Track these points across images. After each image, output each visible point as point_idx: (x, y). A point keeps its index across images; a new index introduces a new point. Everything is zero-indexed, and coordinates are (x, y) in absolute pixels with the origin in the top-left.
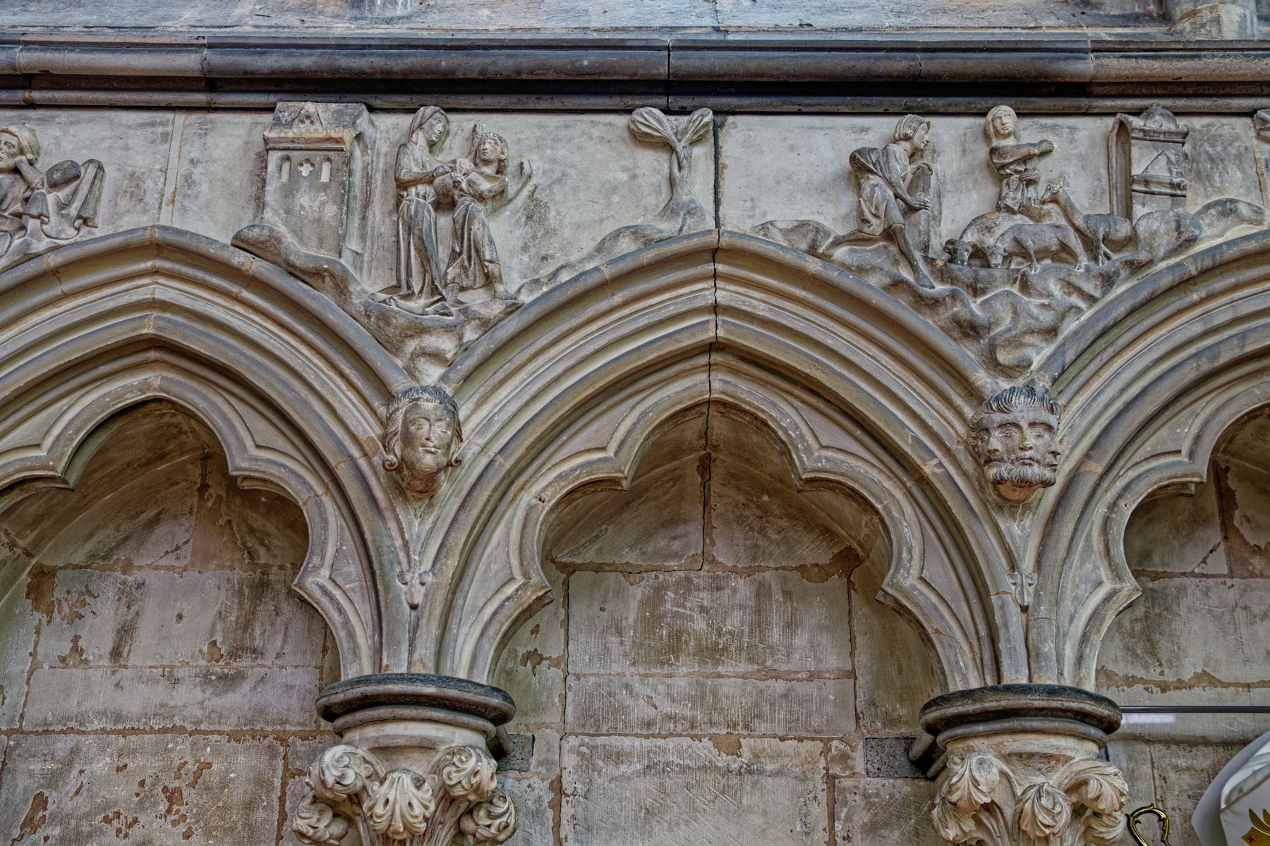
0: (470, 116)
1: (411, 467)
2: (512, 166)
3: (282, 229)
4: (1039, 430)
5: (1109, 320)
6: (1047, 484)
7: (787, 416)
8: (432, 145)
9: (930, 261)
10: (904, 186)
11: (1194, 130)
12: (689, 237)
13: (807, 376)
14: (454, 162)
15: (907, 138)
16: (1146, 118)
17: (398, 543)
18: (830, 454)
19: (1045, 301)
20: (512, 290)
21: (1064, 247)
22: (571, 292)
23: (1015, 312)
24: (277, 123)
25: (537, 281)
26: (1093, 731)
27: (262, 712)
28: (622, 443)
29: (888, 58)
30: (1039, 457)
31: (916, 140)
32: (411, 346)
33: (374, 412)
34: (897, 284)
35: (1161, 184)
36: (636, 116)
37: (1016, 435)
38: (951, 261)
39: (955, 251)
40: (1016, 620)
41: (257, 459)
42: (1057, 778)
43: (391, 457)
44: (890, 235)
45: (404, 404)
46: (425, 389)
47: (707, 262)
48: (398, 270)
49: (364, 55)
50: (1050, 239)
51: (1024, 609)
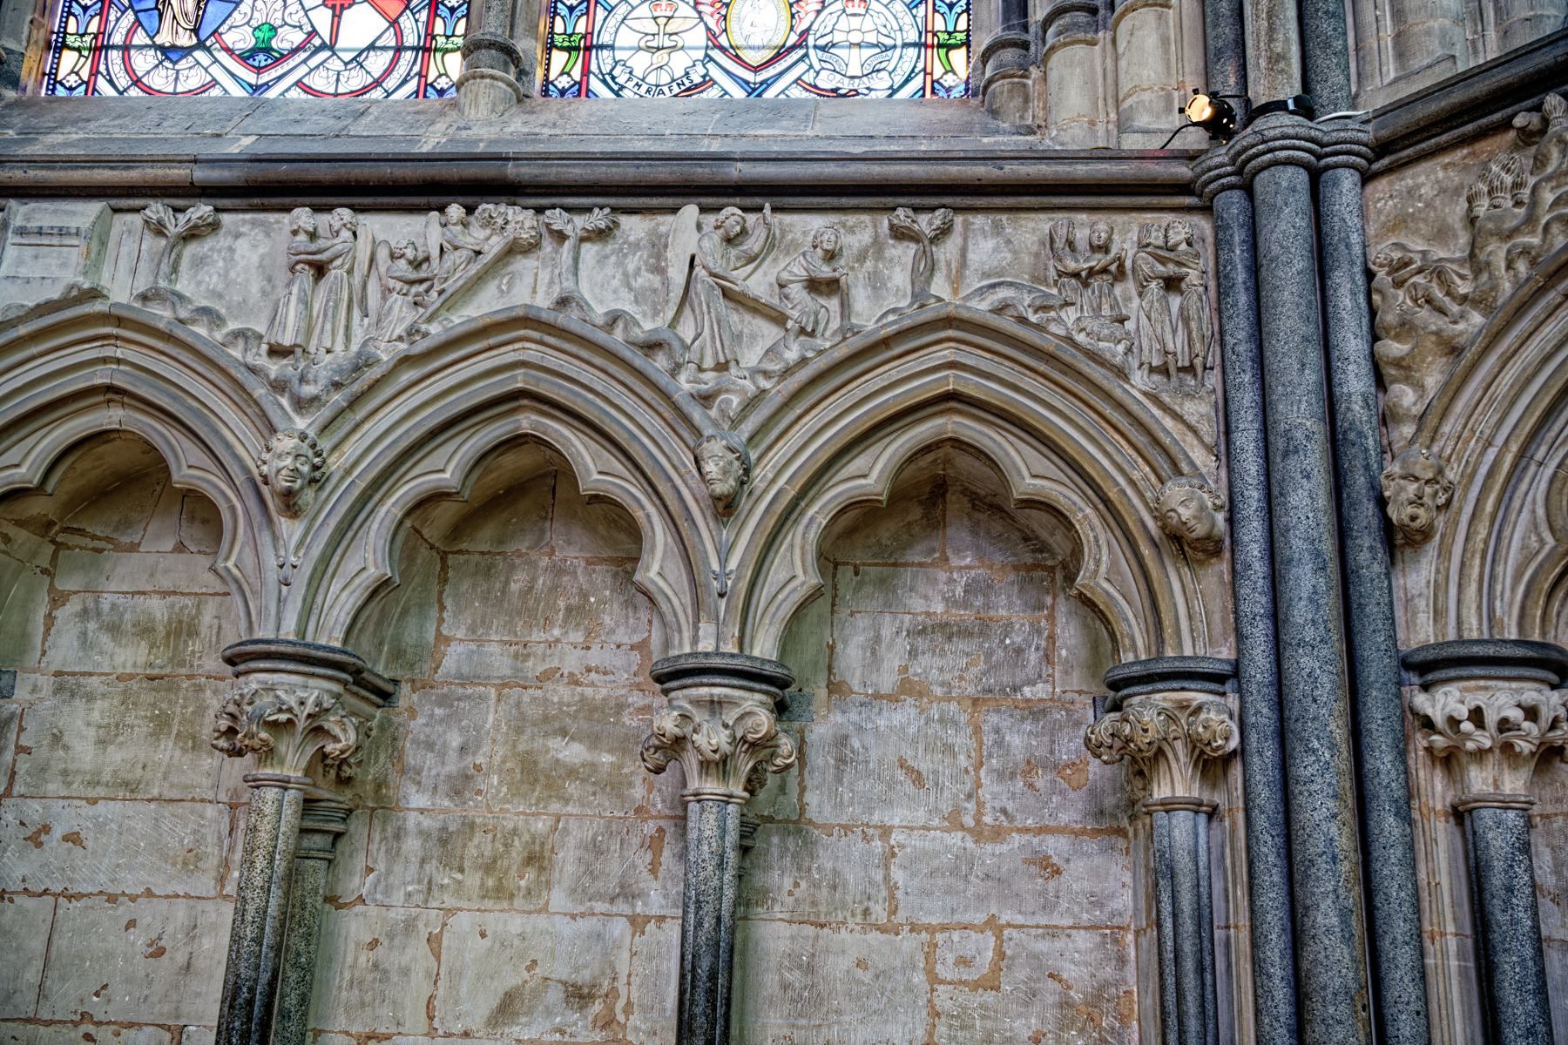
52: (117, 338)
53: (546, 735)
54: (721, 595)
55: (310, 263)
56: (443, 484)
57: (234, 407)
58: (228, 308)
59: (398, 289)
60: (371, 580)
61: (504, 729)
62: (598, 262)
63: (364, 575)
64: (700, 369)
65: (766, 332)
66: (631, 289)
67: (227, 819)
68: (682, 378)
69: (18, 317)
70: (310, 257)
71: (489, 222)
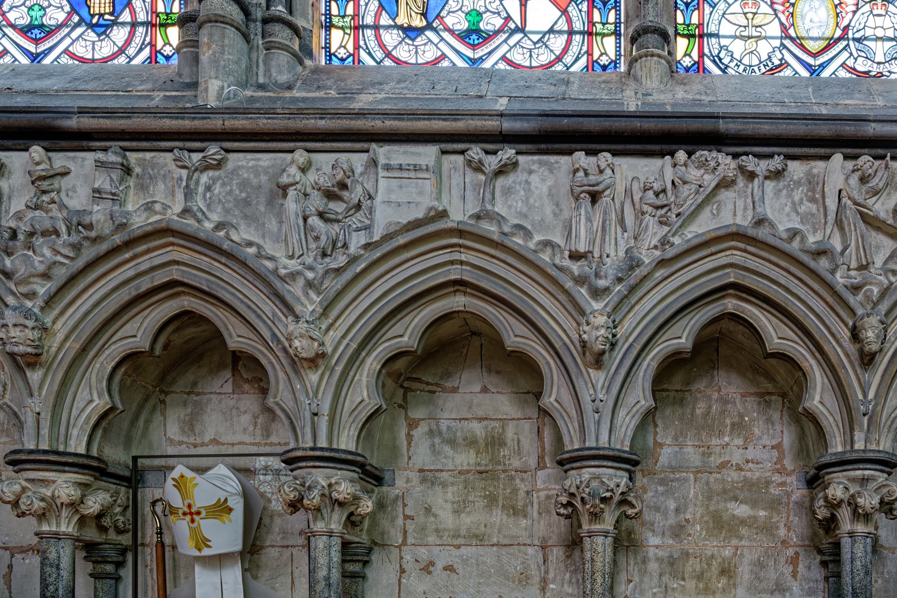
52: (460, 246)
53: (726, 501)
54: (864, 415)
55: (589, 193)
56: (682, 346)
57: (548, 295)
58: (533, 225)
59: (650, 212)
60: (644, 408)
61: (701, 498)
62: (775, 194)
63: (638, 406)
64: (849, 269)
65: (886, 244)
66: (798, 213)
67: (541, 555)
68: (838, 275)
69: (396, 231)
70: (591, 188)
71: (703, 165)
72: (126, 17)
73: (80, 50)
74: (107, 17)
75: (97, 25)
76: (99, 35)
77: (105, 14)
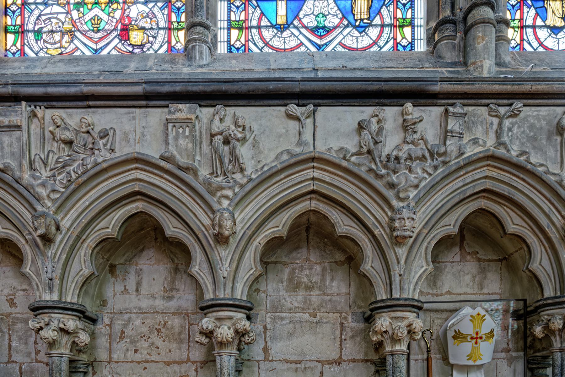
0: (233, 108)
1: (222, 235)
2: (247, 128)
3: (175, 153)
4: (410, 220)
5: (434, 182)
6: (411, 237)
7: (334, 215)
8: (221, 120)
9: (381, 162)
10: (375, 133)
11: (469, 112)
12: (305, 154)
13: (341, 202)
14: (229, 126)
15: (377, 116)
16: (454, 108)
17: (218, 258)
18: (347, 227)
19: (416, 176)
20: (249, 173)
21: (424, 156)
22: (268, 174)
23: (406, 180)
24: (170, 112)
25: (257, 170)
26: (416, 310)
27: (180, 307)
28: (284, 225)
29: (372, 84)
30: (409, 229)
31: (380, 116)
32: (219, 194)
33: (209, 216)
34: (370, 170)
35: (456, 133)
36: (288, 108)
37: (403, 222)
38: (388, 161)
39: (390, 158)
40: (398, 278)
41: (174, 232)
42: (405, 323)
43: (215, 232)
44: (369, 152)
45: (218, 214)
46: (224, 209)
47: (311, 162)
48: (213, 167)
49: (197, 85)
50: (420, 154)
51: (400, 275)
72: (377, 21)
73: (348, 42)
74: (365, 21)
75: (359, 26)
76: (360, 33)
77: (364, 19)
